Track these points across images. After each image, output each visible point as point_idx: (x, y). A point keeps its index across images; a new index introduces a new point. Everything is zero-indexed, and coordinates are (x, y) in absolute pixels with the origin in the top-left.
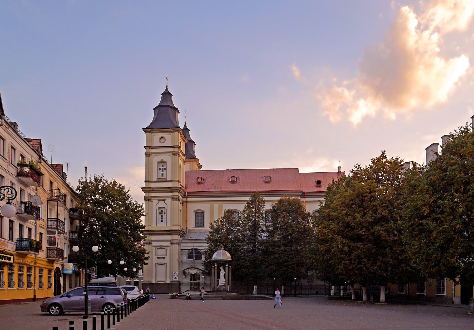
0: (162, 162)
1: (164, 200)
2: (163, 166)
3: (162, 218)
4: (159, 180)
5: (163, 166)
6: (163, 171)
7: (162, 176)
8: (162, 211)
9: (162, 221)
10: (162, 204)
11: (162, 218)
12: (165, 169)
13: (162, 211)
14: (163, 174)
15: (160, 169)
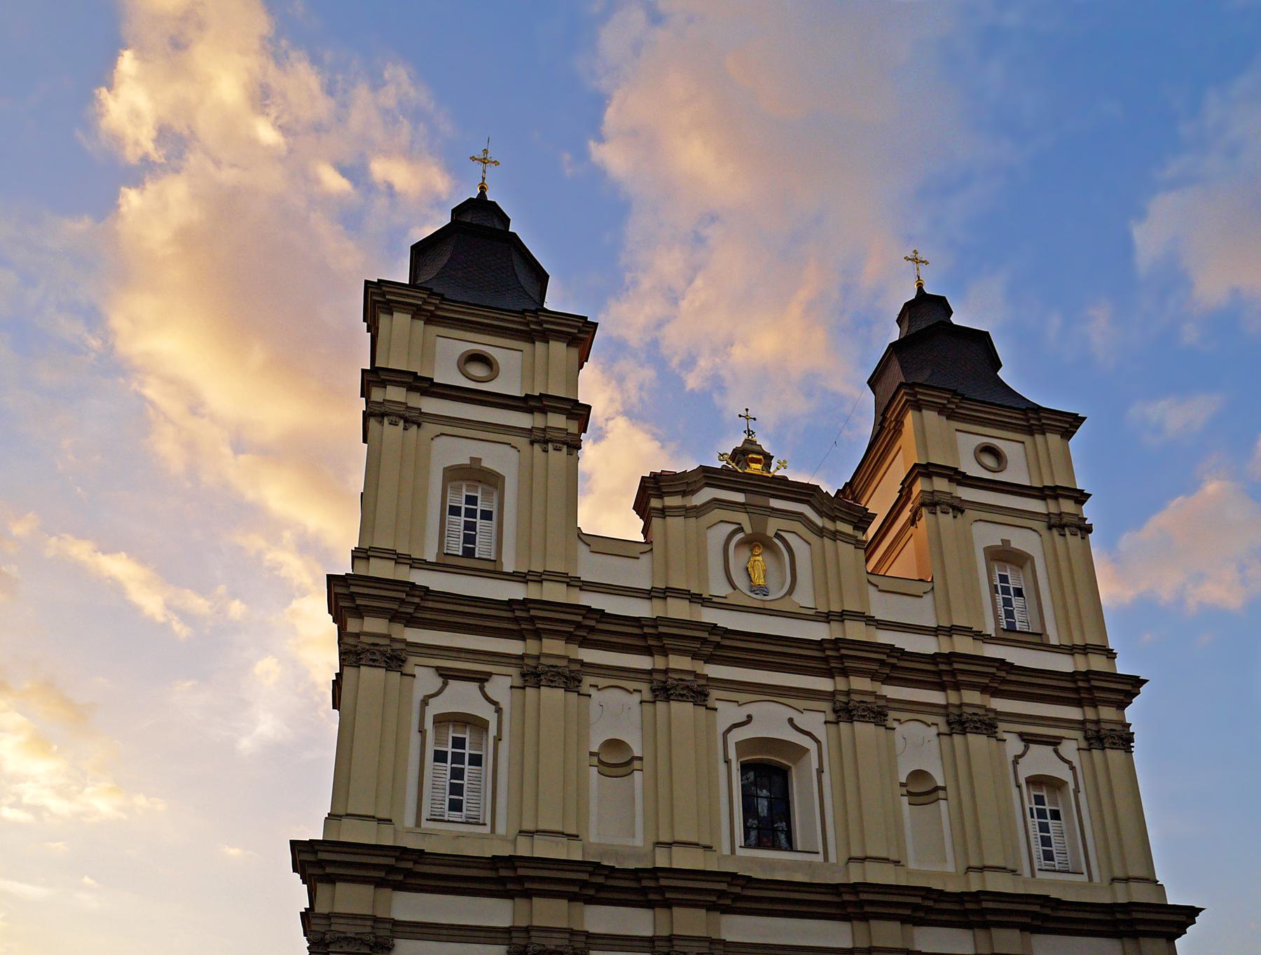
0: (474, 474)
1: (481, 679)
2: (471, 500)
3: (456, 789)
4: (450, 561)
5: (471, 500)
6: (470, 526)
7: (469, 553)
8: (459, 743)
9: (456, 806)
10: (462, 697)
11: (456, 789)
12: (487, 515)
13: (459, 743)
14: (469, 539)
15: (455, 511)
